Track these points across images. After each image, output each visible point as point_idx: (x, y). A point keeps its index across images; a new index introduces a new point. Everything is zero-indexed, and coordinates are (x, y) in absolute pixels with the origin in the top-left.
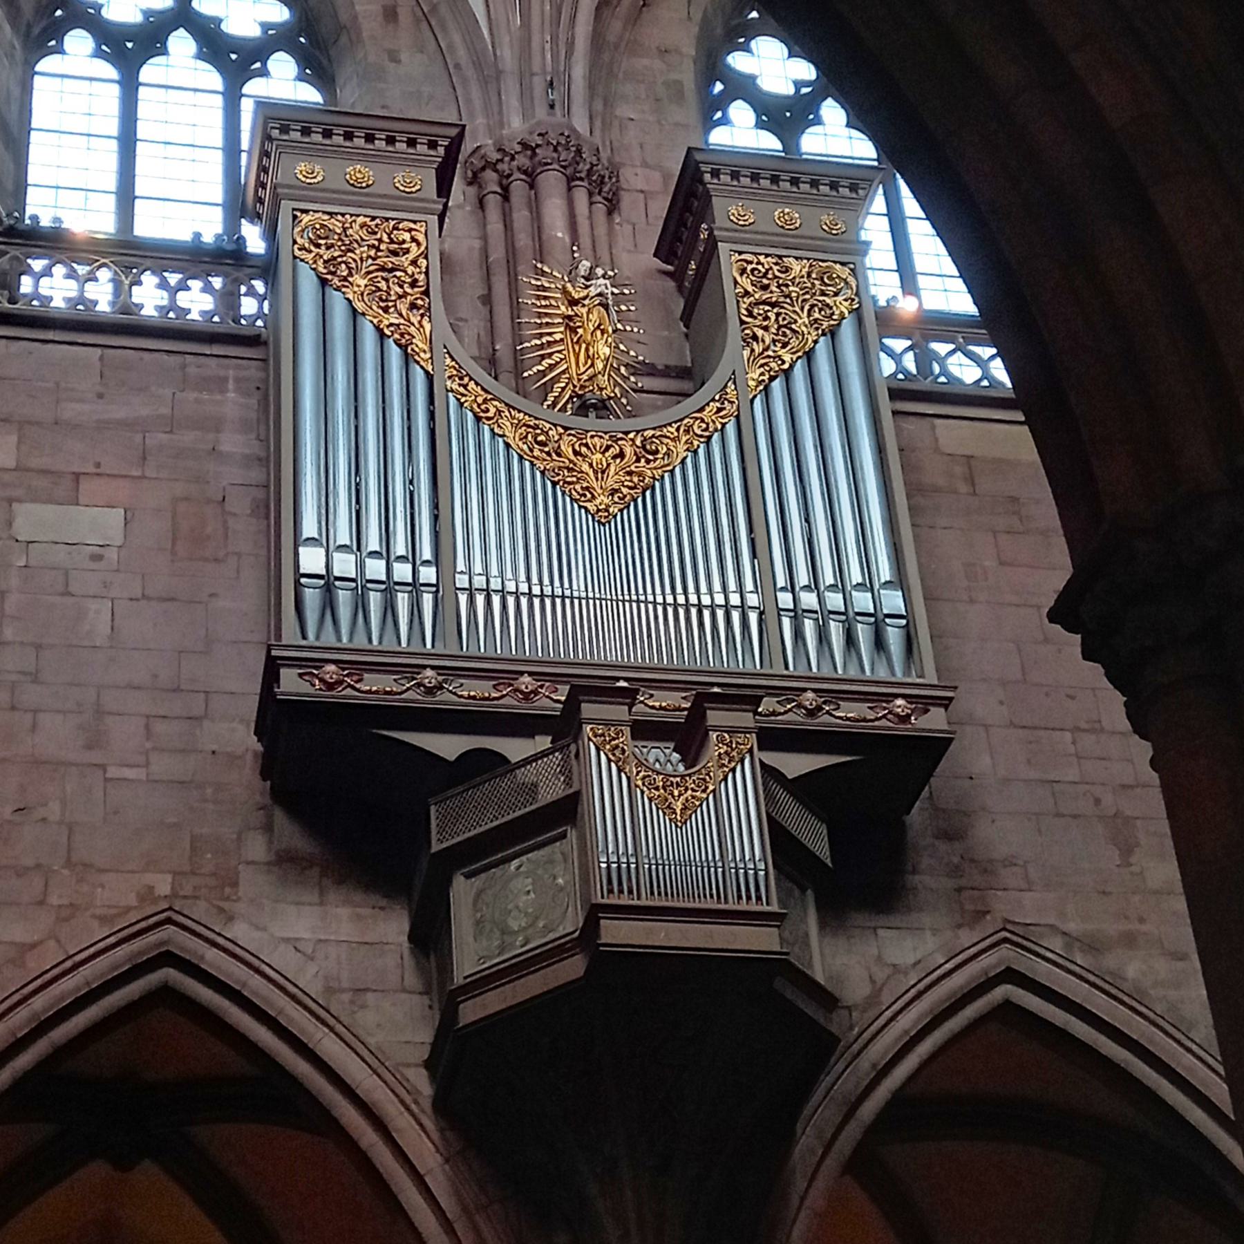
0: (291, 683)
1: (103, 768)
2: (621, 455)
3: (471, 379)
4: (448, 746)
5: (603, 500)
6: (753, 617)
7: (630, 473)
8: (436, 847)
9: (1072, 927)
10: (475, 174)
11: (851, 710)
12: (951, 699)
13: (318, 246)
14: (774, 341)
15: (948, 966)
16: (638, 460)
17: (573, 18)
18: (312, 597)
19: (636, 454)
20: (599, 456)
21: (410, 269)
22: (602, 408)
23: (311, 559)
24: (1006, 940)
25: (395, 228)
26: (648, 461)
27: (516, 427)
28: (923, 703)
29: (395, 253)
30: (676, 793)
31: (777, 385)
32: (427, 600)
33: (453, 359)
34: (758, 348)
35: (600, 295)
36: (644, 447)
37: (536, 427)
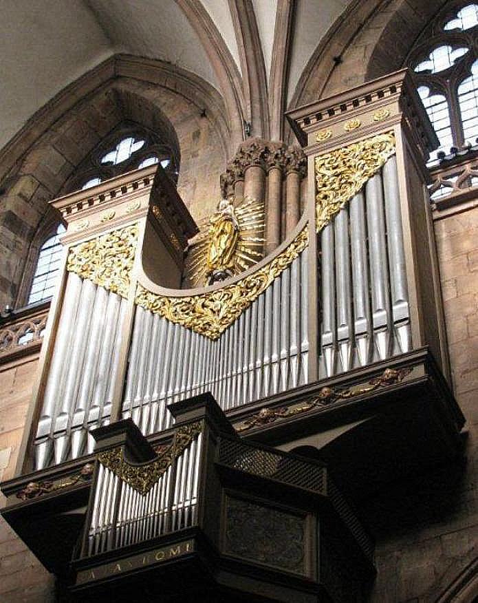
19: (241, 292)
22: (224, 276)
34: (325, 202)
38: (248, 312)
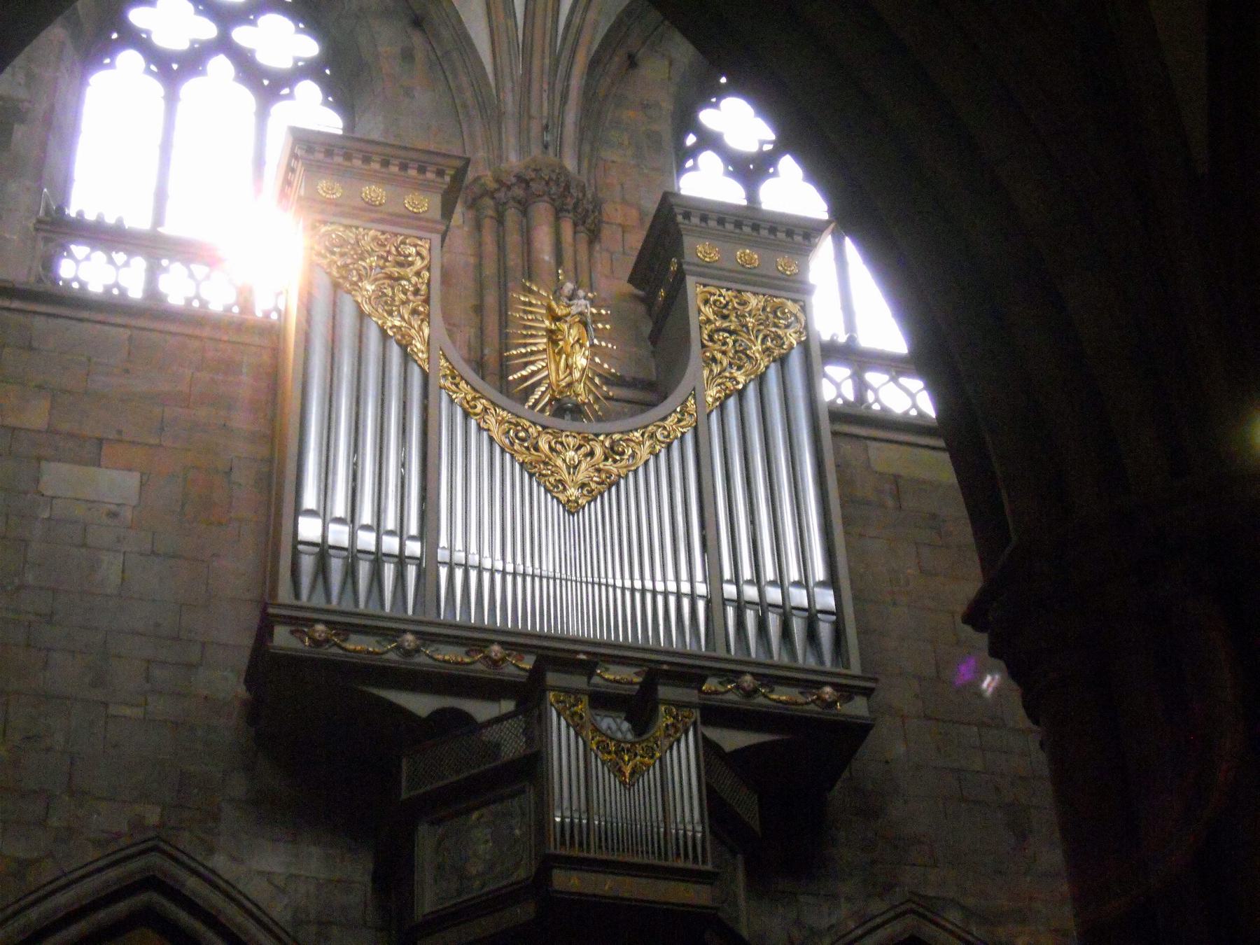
0: (282, 637)
1: (106, 705)
2: (591, 454)
3: (462, 378)
4: (421, 704)
5: (573, 492)
6: (701, 605)
7: (599, 470)
8: (404, 796)
9: (970, 902)
10: (474, 200)
11: (782, 694)
12: (872, 690)
13: (333, 253)
14: (730, 364)
15: (859, 932)
16: (606, 459)
17: (568, 76)
18: (307, 563)
20: (571, 453)
21: (414, 279)
23: (309, 529)
24: (912, 911)
25: (403, 243)
26: (615, 461)
27: (500, 423)
28: (847, 692)
29: (401, 265)
30: (626, 758)
31: (732, 403)
32: (412, 571)
33: (447, 360)
34: (716, 369)
35: (581, 314)
36: (612, 448)
37: (517, 424)
38: (614, 489)
